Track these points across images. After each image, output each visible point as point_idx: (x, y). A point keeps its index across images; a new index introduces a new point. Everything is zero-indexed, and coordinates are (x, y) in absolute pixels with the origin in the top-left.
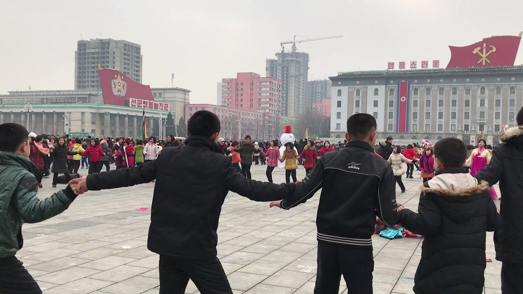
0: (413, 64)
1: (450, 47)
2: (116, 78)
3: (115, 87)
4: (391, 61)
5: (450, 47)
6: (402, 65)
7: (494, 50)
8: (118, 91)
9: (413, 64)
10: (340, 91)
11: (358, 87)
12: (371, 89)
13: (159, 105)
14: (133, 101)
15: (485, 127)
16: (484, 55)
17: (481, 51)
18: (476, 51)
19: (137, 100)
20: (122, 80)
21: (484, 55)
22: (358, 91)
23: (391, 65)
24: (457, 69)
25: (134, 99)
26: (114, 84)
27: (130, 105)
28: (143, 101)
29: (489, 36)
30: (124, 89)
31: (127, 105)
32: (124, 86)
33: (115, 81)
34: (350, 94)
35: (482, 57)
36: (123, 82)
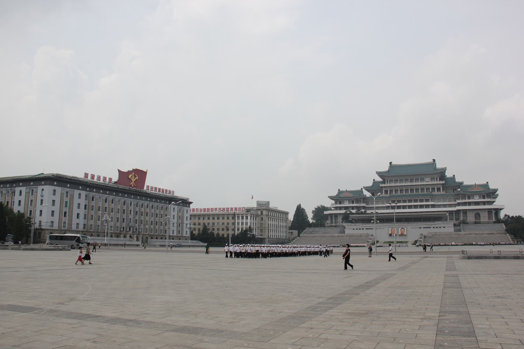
0: (99, 178)
1: (119, 171)
4: (87, 172)
5: (119, 171)
6: (93, 177)
7: (137, 178)
9: (99, 178)
10: (55, 191)
11: (67, 189)
12: (77, 192)
15: (131, 228)
16: (133, 180)
17: (132, 177)
18: (130, 177)
21: (133, 180)
22: (67, 192)
23: (86, 175)
24: (121, 187)
29: (135, 168)
34: (62, 194)
35: (132, 181)
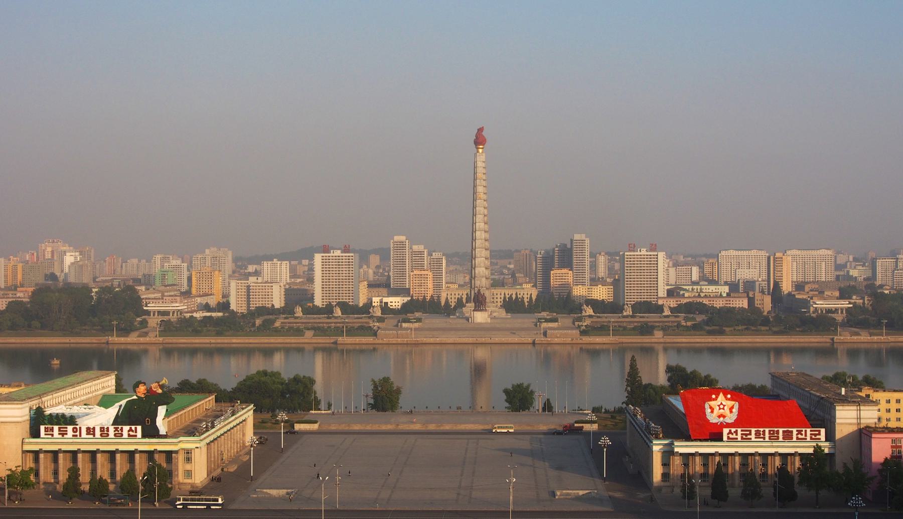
2: (716, 399)
3: (712, 412)
8: (719, 417)
13: (795, 433)
14: (730, 432)
19: (739, 430)
20: (727, 399)
25: (733, 430)
26: (711, 408)
27: (725, 438)
28: (753, 430)
30: (731, 412)
31: (720, 439)
32: (731, 412)
33: (712, 403)
36: (731, 403)
